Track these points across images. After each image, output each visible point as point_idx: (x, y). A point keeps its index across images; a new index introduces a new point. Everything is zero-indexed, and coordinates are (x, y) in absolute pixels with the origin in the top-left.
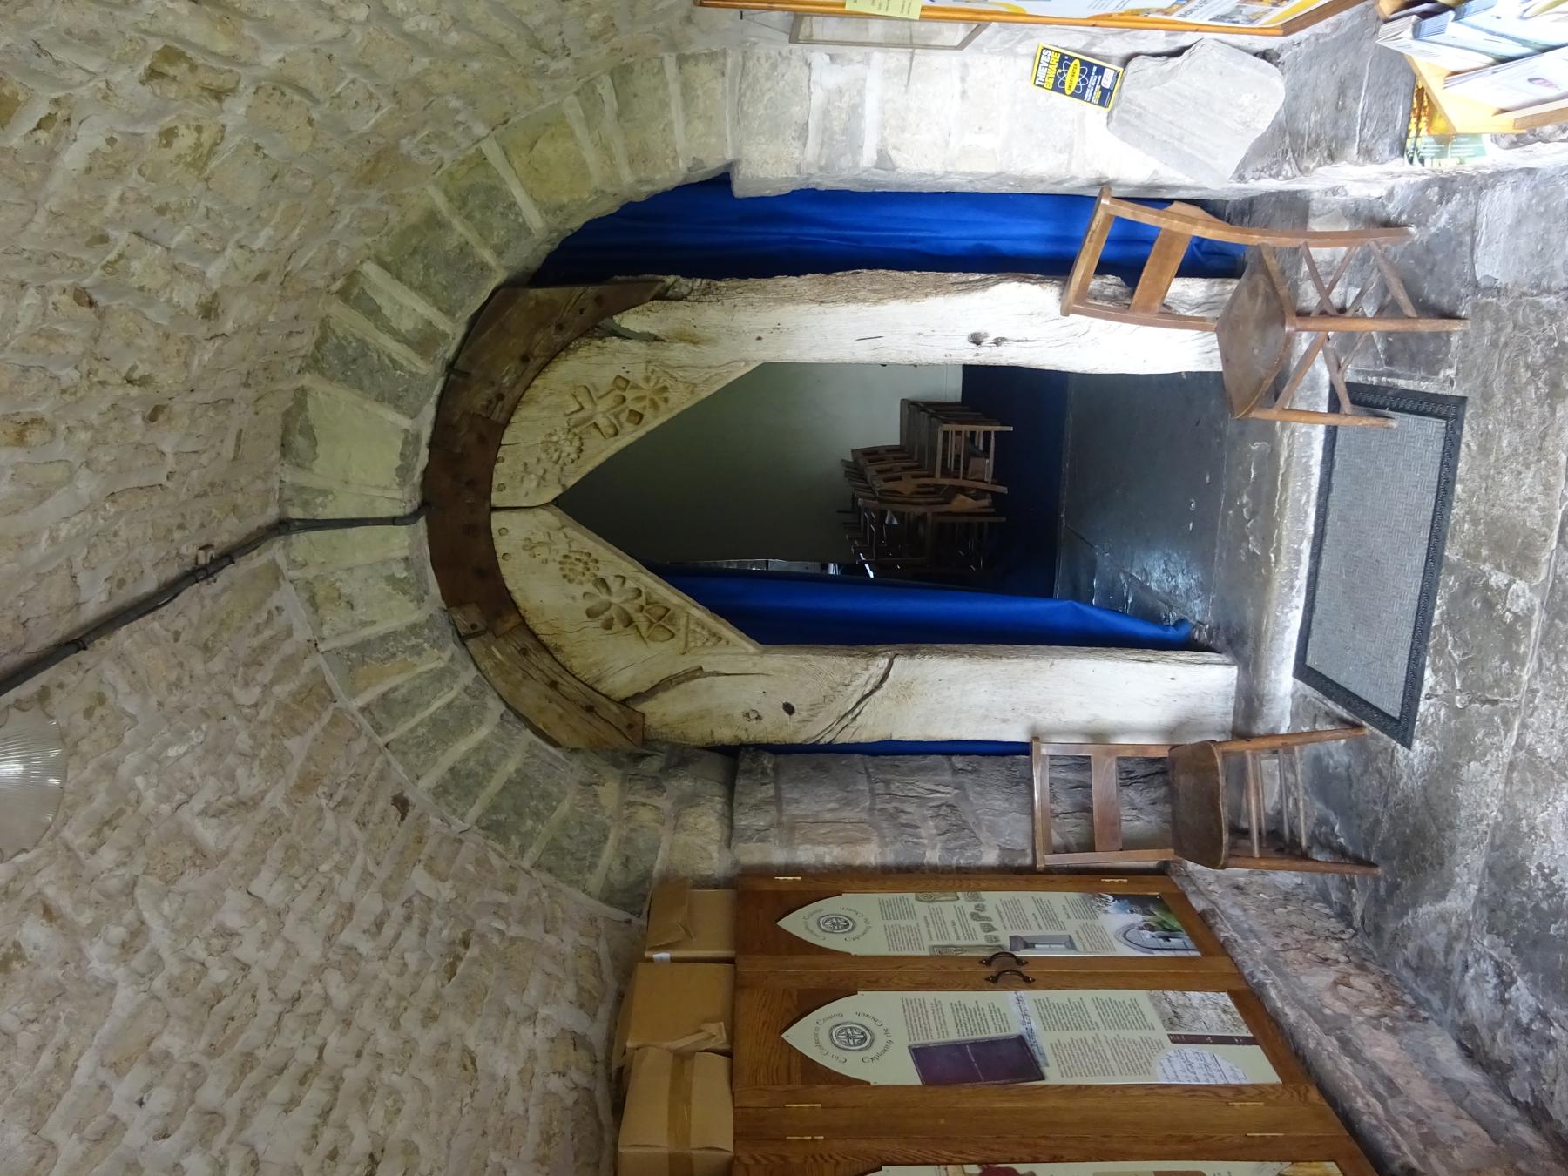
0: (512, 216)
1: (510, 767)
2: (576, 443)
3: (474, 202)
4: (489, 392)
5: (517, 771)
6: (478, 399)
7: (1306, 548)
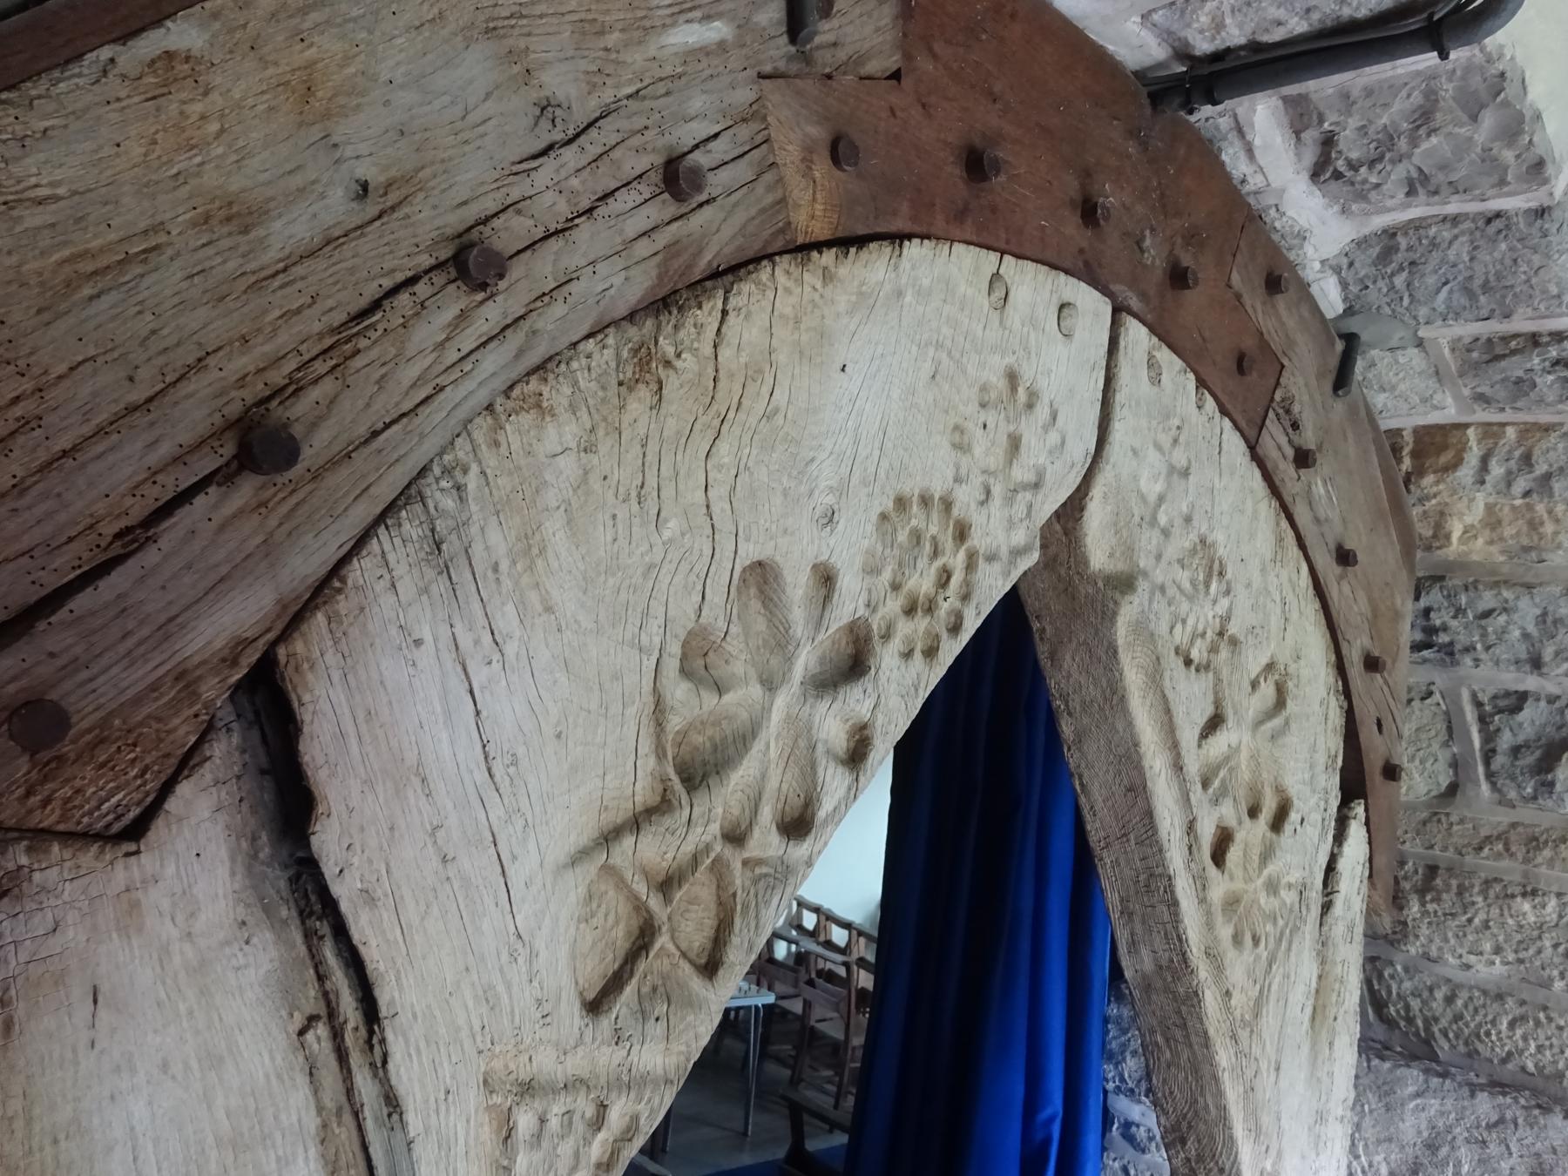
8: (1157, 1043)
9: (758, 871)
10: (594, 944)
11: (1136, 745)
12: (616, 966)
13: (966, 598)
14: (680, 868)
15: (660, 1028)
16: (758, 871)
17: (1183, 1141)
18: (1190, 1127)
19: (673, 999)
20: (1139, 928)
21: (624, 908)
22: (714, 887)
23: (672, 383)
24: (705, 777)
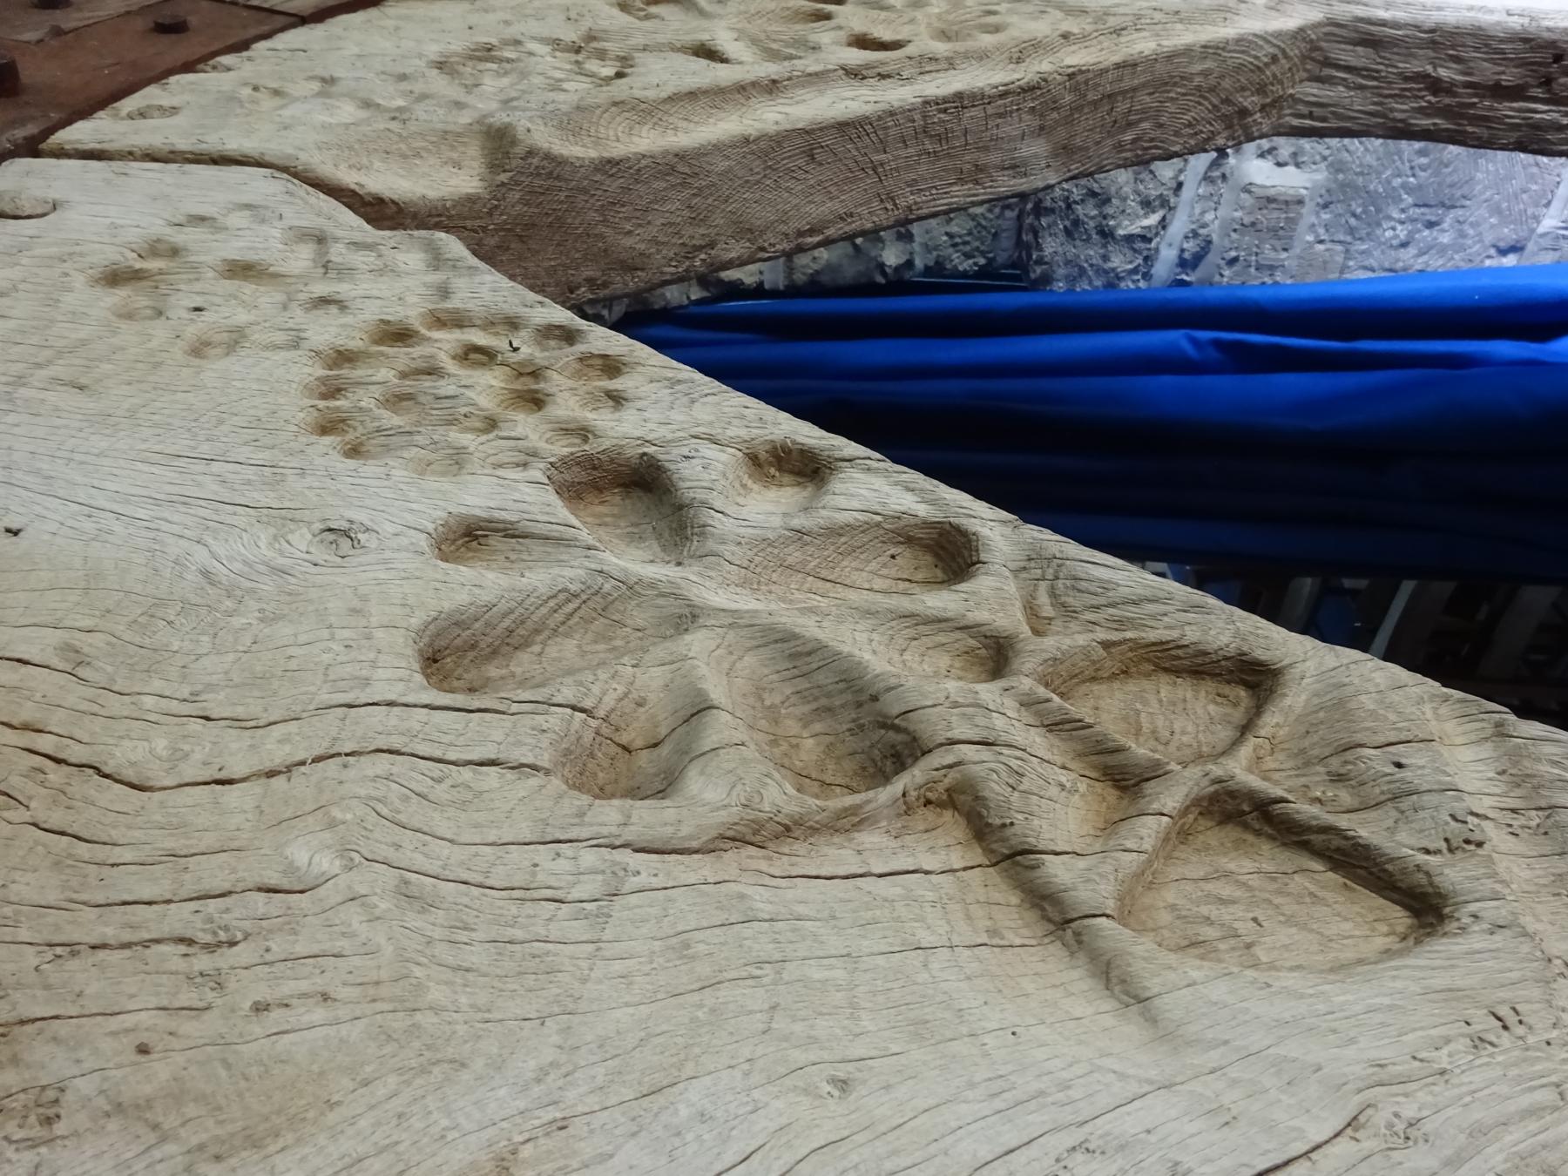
8: (1134, 141)
9: (1048, 611)
10: (1290, 921)
11: (746, 140)
12: (1317, 866)
13: (513, 324)
14: (1080, 755)
15: (1414, 757)
16: (1048, 611)
17: (1244, 113)
18: (1227, 101)
19: (1346, 739)
20: (994, 158)
21: (1192, 865)
22: (1095, 687)
24: (886, 724)
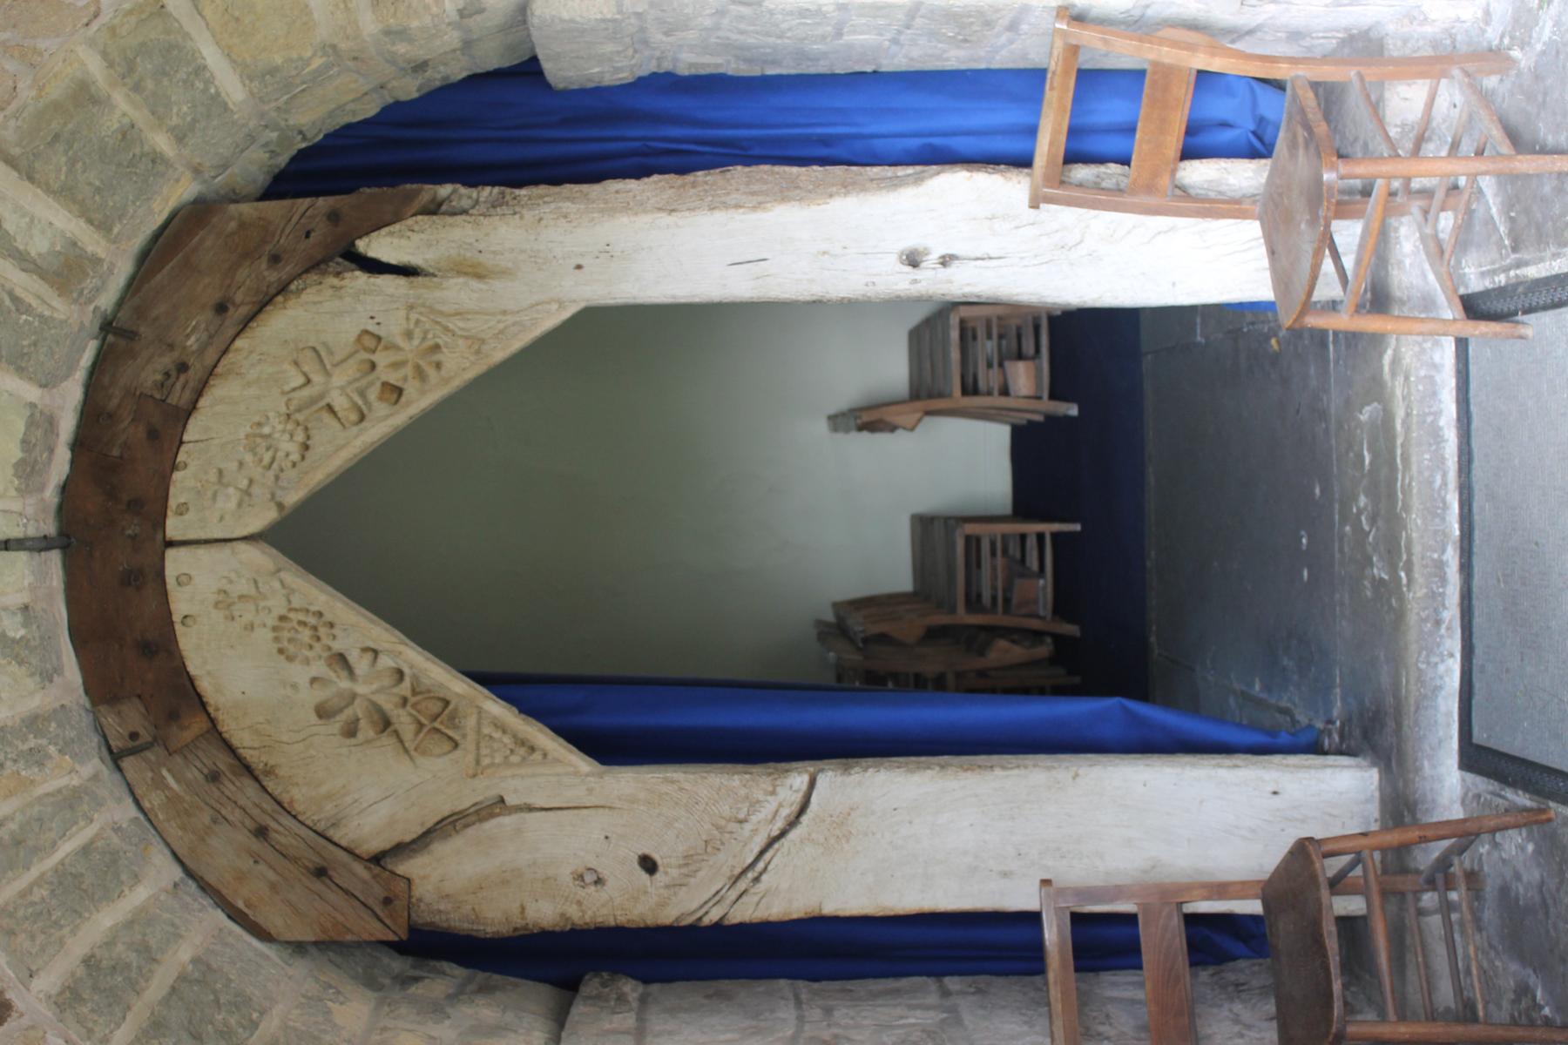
0: (199, 85)
1: (184, 954)
2: (300, 437)
3: (145, 66)
4: (166, 361)
5: (196, 961)
6: (148, 372)
7: (1452, 557)
23: (272, 762)
